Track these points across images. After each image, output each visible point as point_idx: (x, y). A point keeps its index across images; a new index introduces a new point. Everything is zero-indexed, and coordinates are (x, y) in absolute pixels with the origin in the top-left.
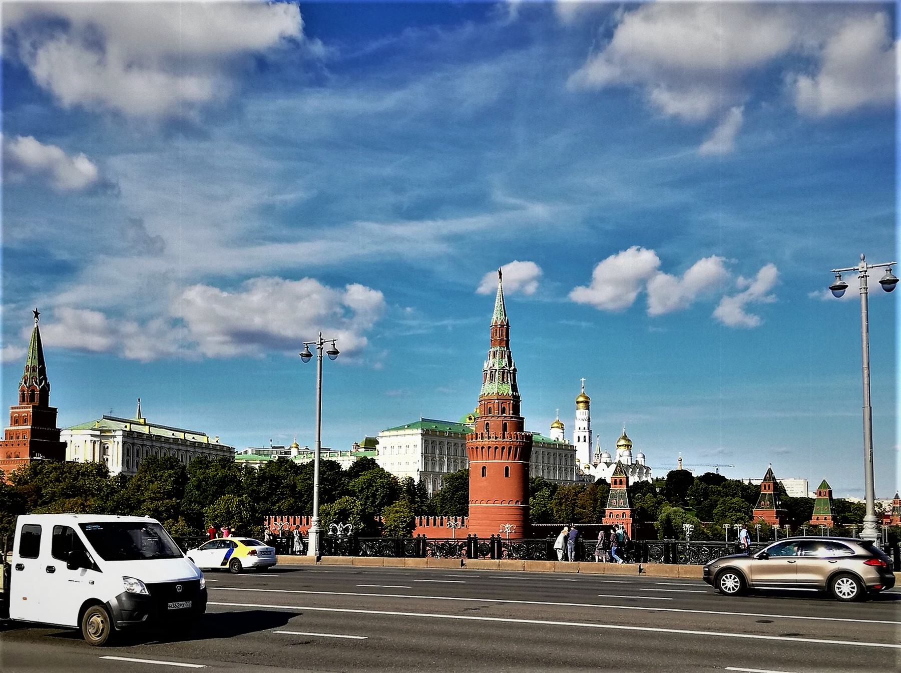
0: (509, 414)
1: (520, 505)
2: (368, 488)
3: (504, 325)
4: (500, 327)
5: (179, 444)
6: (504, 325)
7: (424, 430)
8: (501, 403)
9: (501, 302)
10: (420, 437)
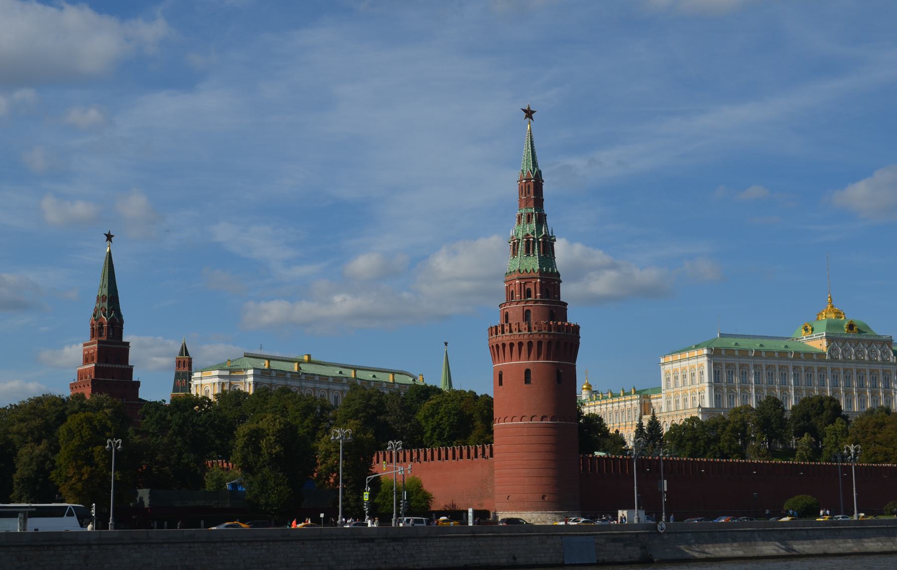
0: (536, 297)
1: (549, 422)
2: (432, 415)
3: (531, 179)
4: (525, 182)
5: (329, 383)
6: (531, 179)
7: (712, 349)
8: (525, 284)
9: (528, 148)
10: (706, 358)
